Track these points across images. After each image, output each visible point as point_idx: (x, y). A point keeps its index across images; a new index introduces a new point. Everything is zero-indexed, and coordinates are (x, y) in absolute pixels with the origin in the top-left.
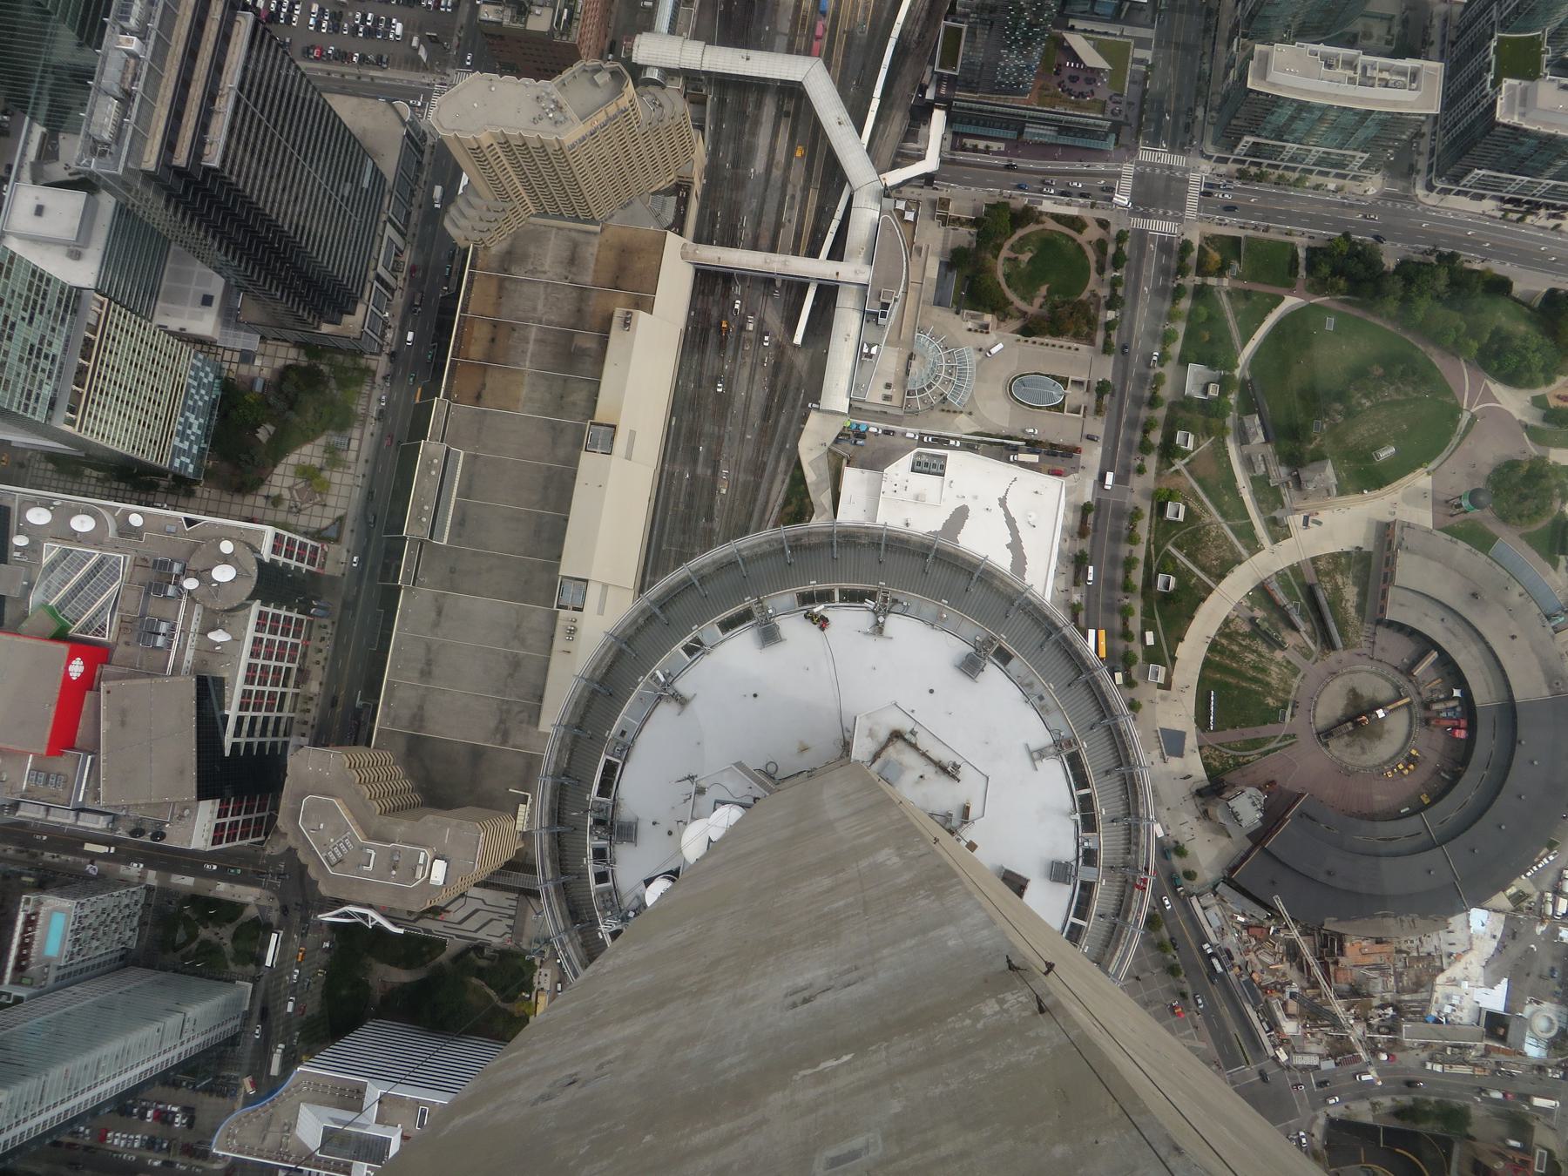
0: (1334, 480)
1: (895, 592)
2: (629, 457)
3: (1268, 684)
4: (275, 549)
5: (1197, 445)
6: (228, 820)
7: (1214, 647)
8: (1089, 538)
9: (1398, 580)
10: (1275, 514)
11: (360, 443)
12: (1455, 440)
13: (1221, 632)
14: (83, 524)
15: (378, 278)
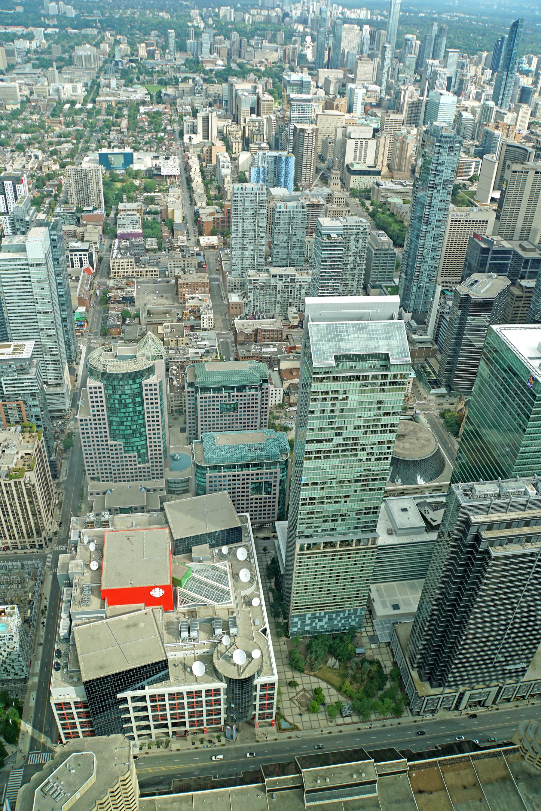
4: (264, 686)
6: (74, 711)
14: (244, 575)
15: (462, 694)
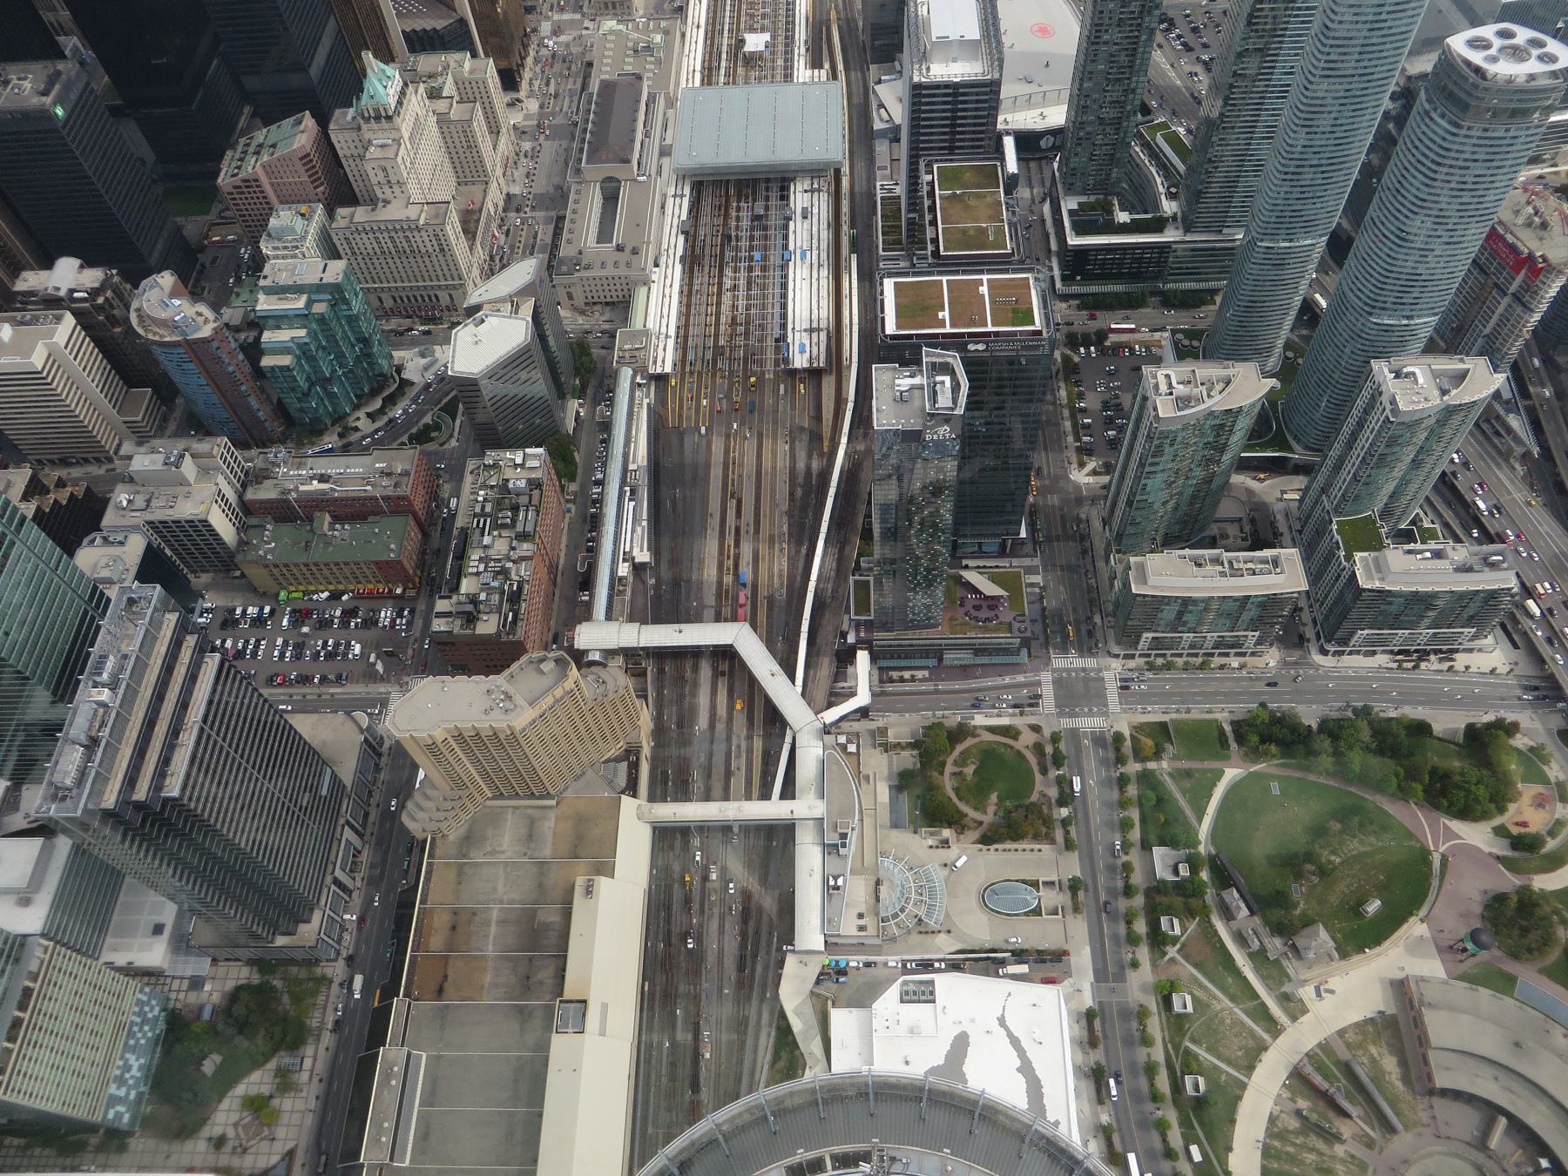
0: (1332, 944)
1: (892, 1149)
2: (602, 1033)
5: (1184, 929)
7: (1267, 1152)
8: (1101, 1046)
9: (1434, 1040)
10: (1284, 989)
11: (314, 1060)
12: (1435, 883)
15: (336, 882)
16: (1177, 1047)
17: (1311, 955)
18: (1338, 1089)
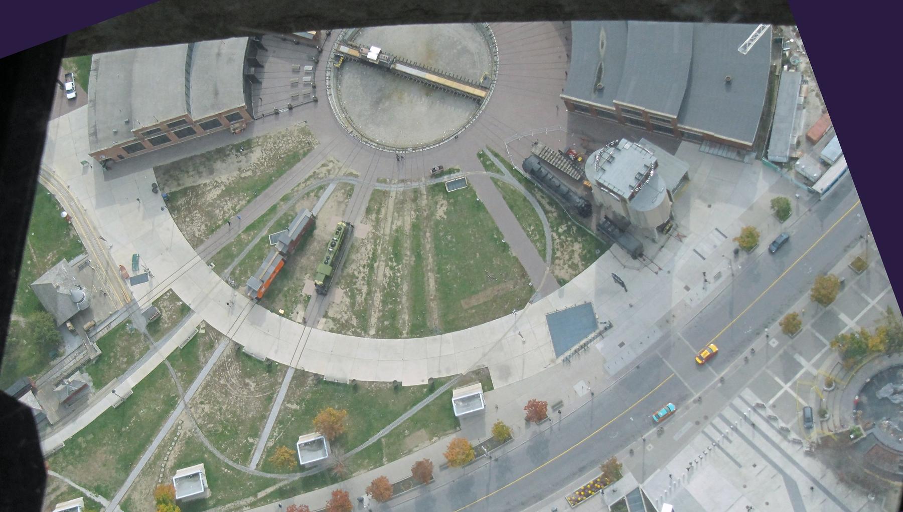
0: (62, 265)
3: (415, 227)
5: (72, 493)
7: (389, 330)
10: (143, 329)
13: (362, 329)
16: (267, 483)
17: (81, 293)
18: (275, 240)
